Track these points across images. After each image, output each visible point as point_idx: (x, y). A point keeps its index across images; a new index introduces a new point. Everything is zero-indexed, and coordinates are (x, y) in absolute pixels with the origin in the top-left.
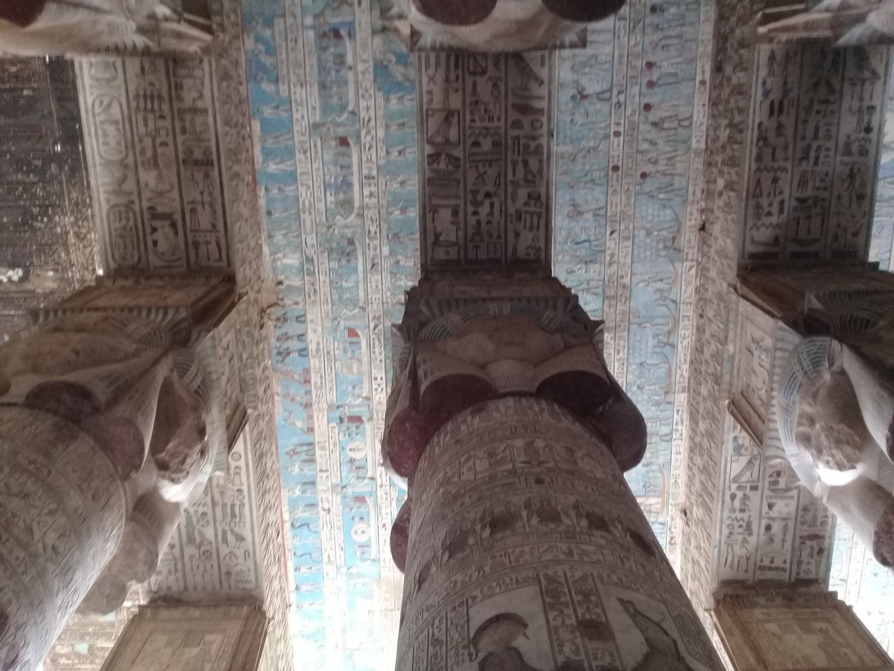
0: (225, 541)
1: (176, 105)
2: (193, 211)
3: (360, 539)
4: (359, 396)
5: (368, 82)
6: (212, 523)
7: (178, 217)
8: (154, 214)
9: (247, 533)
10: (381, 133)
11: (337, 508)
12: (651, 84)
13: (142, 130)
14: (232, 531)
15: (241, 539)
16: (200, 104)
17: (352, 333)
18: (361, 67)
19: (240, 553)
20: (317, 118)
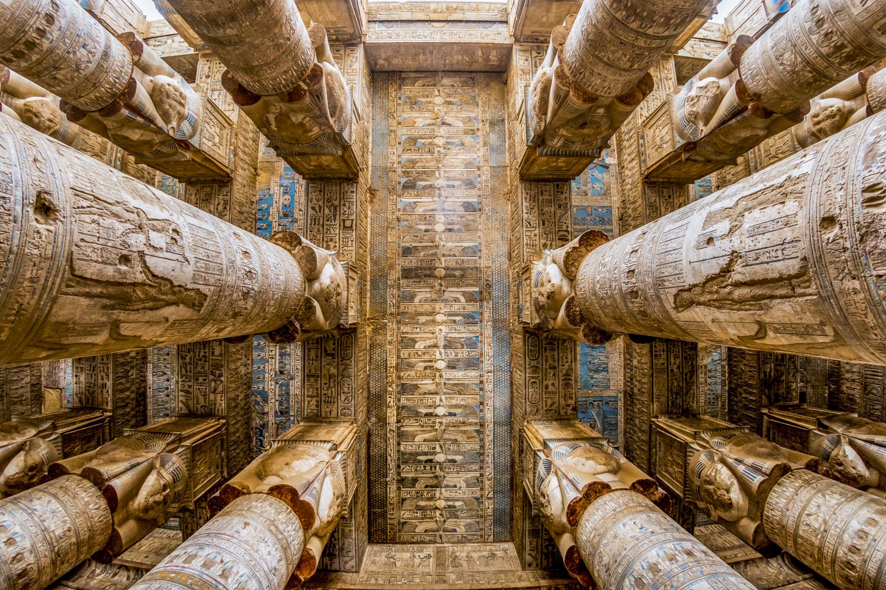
0: (320, 207)
1: (319, 399)
2: (317, 357)
3: (287, 197)
5: (271, 395)
7: (324, 354)
8: (332, 355)
9: (310, 211)
10: (267, 375)
11: (296, 211)
12: (167, 389)
13: (333, 390)
15: (313, 208)
16: (310, 399)
18: (273, 401)
19: (314, 201)
20: (291, 382)
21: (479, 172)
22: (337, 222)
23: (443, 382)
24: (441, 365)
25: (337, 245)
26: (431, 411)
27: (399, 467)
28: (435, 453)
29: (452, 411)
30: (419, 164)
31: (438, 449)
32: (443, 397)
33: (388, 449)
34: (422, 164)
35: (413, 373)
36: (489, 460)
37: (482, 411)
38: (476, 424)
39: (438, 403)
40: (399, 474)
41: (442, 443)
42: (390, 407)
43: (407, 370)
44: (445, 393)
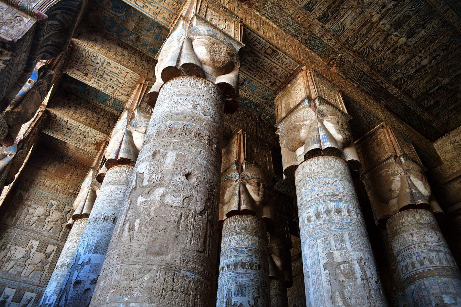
4: (248, 90)
6: (252, 62)
14: (245, 65)
17: (266, 99)
22: (263, 57)
23: (412, 48)
24: (403, 40)
25: (278, 67)
26: (418, 67)
32: (421, 55)
33: (406, 103)
35: (386, 62)
42: (388, 87)
43: (381, 64)
44: (419, 52)
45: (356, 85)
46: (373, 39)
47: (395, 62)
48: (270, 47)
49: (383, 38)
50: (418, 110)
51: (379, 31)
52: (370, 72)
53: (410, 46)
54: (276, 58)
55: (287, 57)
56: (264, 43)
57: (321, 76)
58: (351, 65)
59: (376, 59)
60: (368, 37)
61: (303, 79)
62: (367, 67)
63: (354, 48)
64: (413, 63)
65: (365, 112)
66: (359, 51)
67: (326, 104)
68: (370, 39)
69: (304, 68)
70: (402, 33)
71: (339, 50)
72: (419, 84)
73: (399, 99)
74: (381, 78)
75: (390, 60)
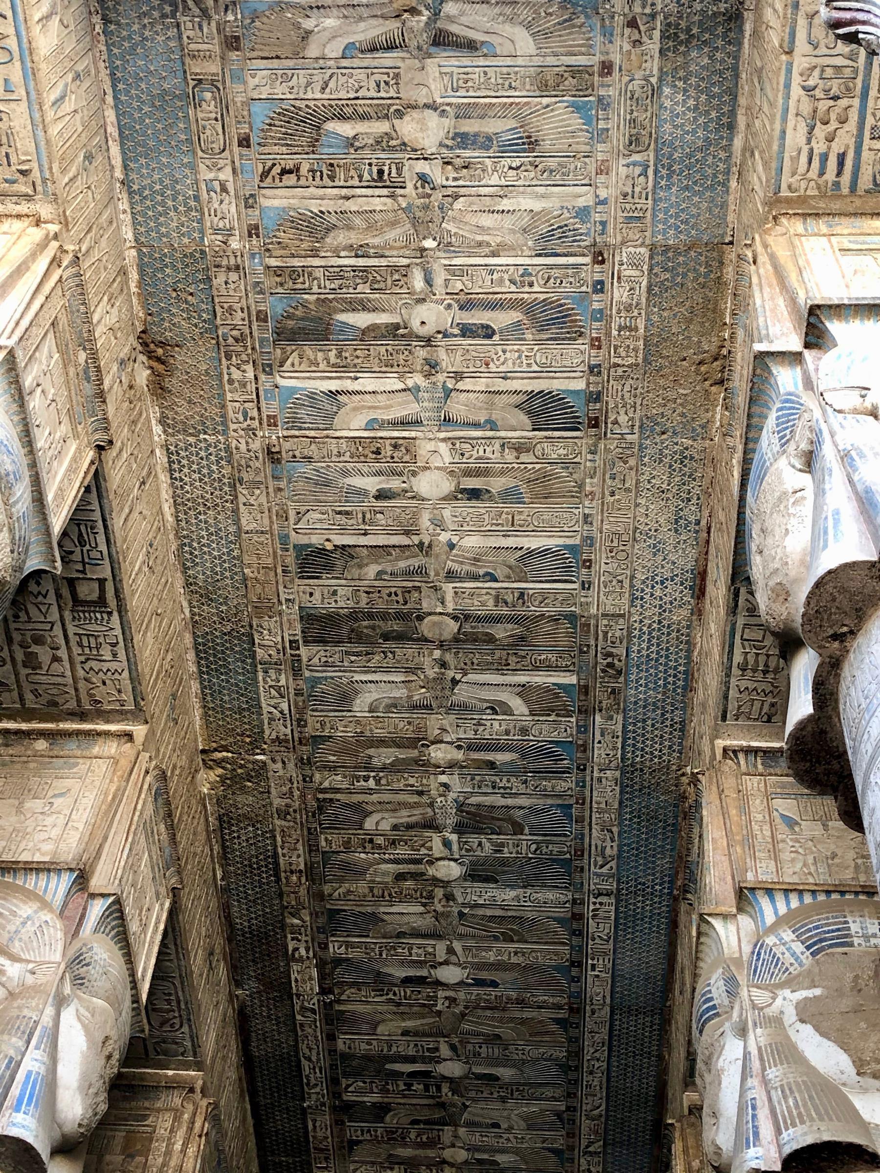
21: (597, 273)
23: (456, 910)
24: (451, 870)
26: (424, 973)
27: (335, 1081)
28: (439, 1061)
29: (484, 975)
30: (340, 238)
31: (445, 1051)
32: (457, 946)
33: (303, 1047)
34: (354, 238)
35: (362, 887)
36: (596, 1081)
37: (576, 980)
38: (559, 1007)
39: (441, 956)
40: (337, 1095)
41: (455, 1040)
42: (301, 960)
43: (341, 880)
44: (461, 937)
45: (222, 879)
46: (386, 797)
47: (382, 909)
48: (102, 582)
49: (413, 819)
50: (318, 1090)
51: (420, 793)
52: (294, 878)
53: (454, 900)
54: (86, 627)
55: (122, 655)
56: (95, 554)
57: (168, 803)
58: (261, 812)
59: (342, 856)
60: (378, 782)
61: (109, 775)
62: (299, 856)
63: (317, 777)
64: (420, 951)
65: (179, 1002)
66: (320, 796)
67: (112, 939)
68: (378, 792)
69: (140, 731)
70: (467, 850)
71: (273, 741)
72: (383, 1021)
73: (299, 1017)
74: (308, 918)
75: (375, 891)
